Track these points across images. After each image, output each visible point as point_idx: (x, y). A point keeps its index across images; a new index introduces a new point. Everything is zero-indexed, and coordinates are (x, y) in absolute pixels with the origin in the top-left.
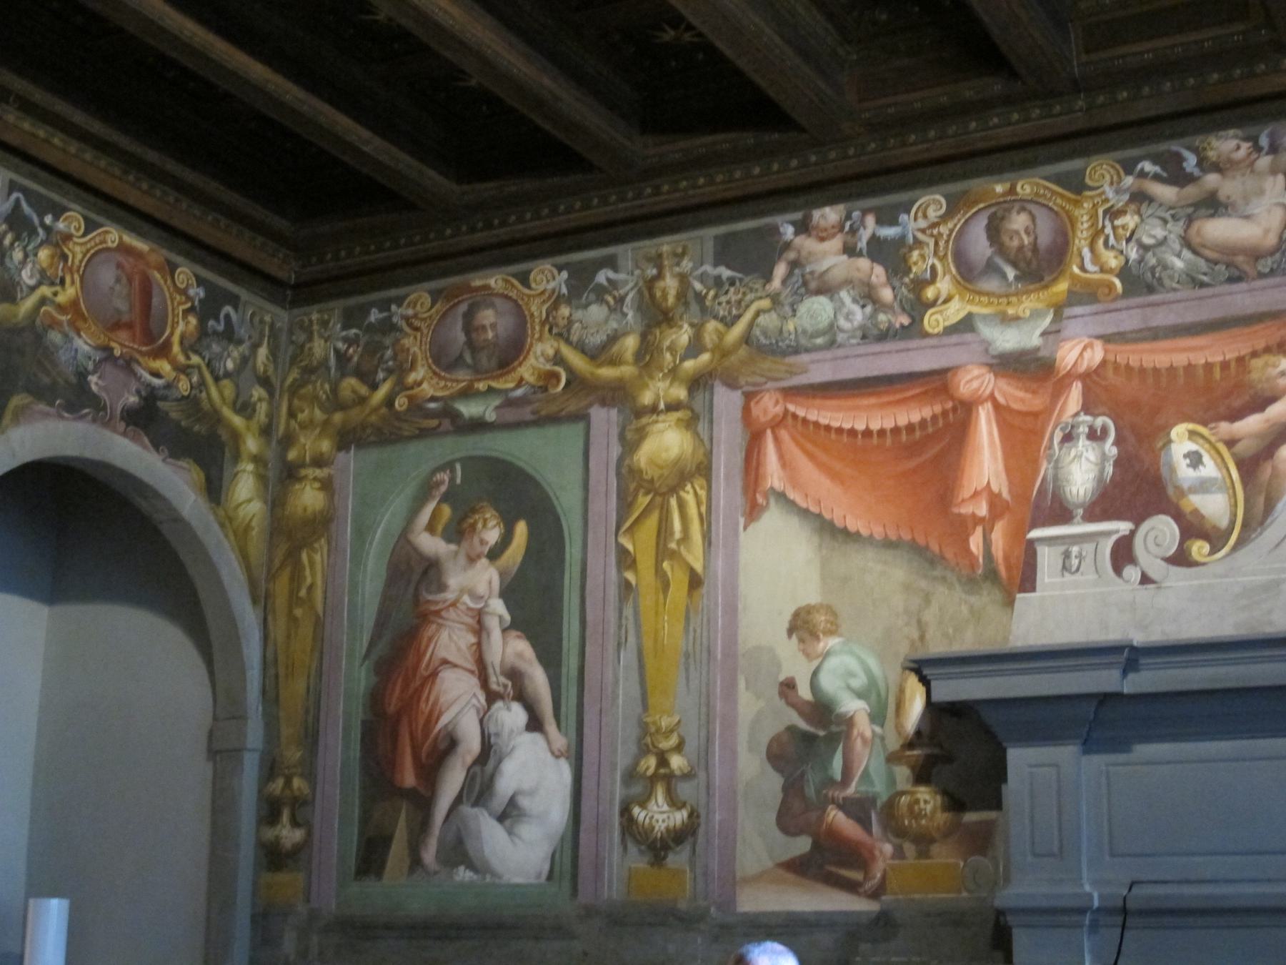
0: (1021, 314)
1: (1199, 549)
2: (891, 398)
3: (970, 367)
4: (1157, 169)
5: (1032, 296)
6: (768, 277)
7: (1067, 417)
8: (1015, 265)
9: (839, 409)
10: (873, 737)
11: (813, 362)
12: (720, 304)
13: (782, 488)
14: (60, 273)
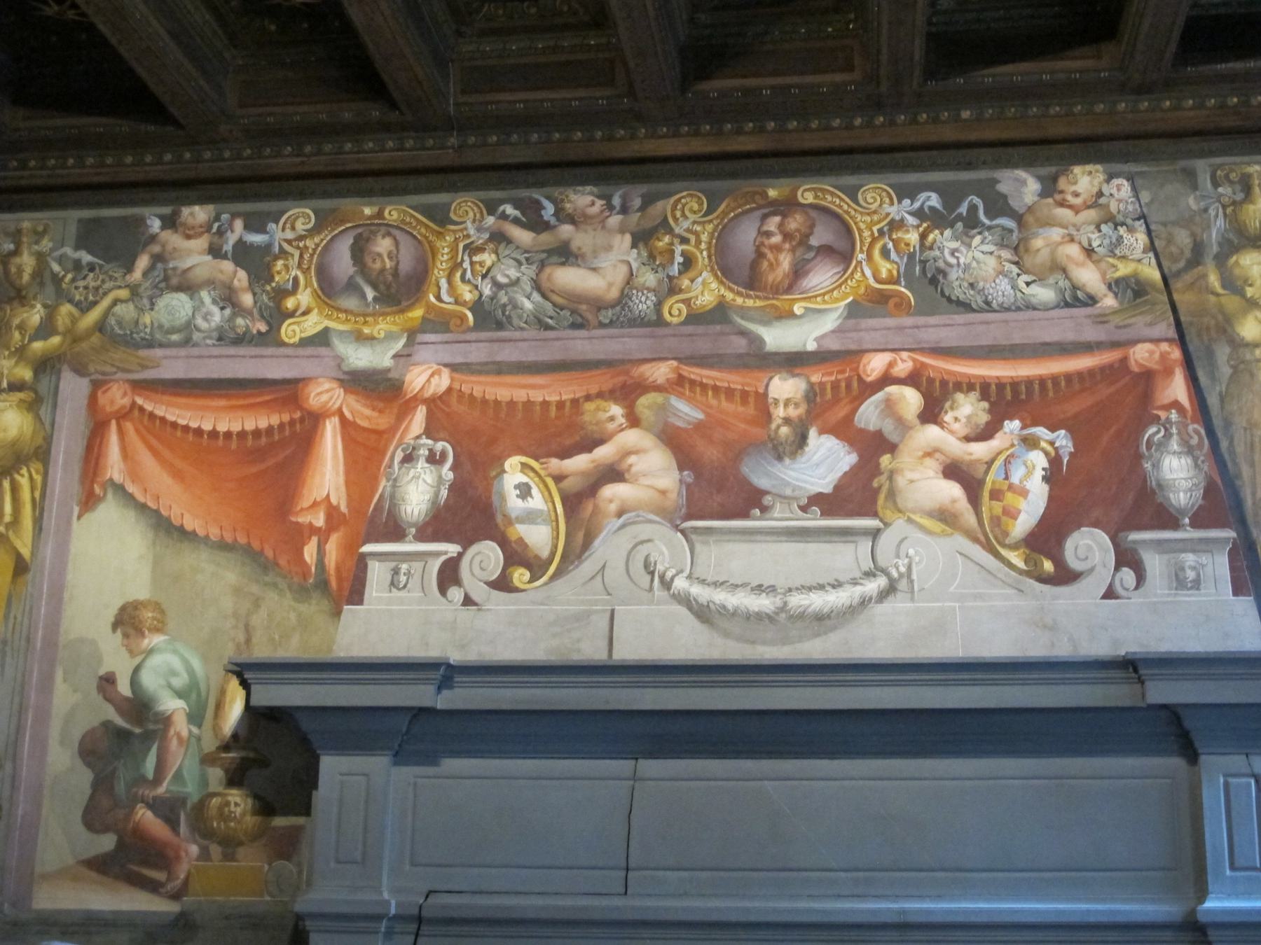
0: (376, 335)
1: (520, 576)
2: (241, 402)
3: (321, 380)
4: (517, 213)
5: (388, 318)
6: (129, 269)
7: (409, 439)
8: (375, 287)
9: (187, 407)
10: (189, 739)
11: (166, 357)
12: (76, 288)
13: (122, 481)
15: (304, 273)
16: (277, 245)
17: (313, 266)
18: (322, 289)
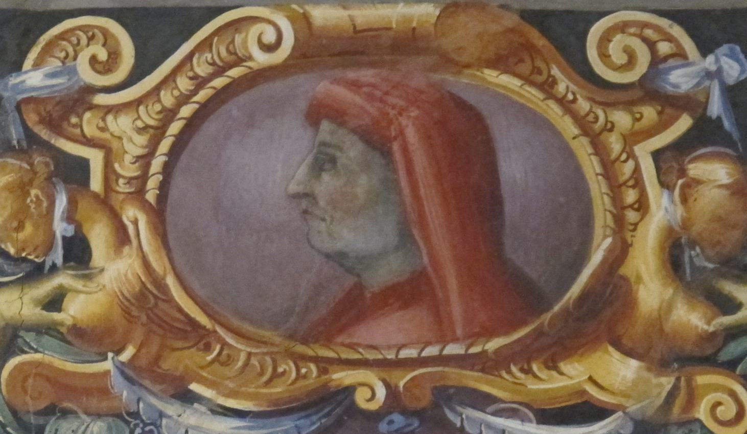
14: (61, 228)
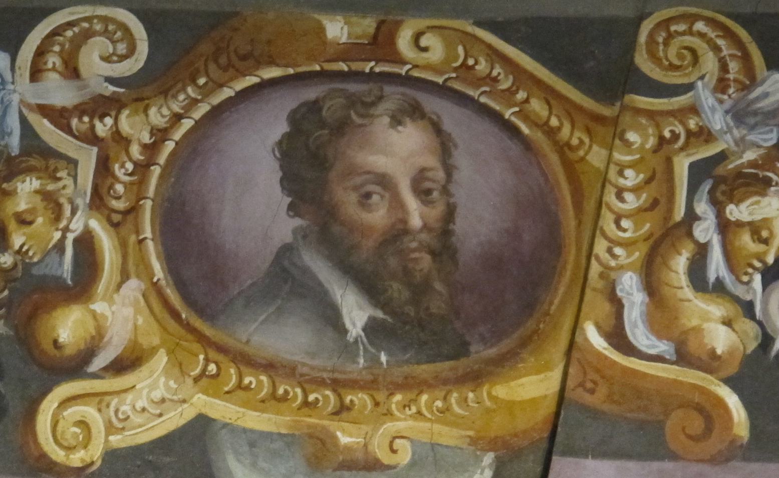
0: (385, 457)
5: (424, 398)
15: (116, 225)
16: (13, 123)
17: (148, 204)
18: (181, 285)
